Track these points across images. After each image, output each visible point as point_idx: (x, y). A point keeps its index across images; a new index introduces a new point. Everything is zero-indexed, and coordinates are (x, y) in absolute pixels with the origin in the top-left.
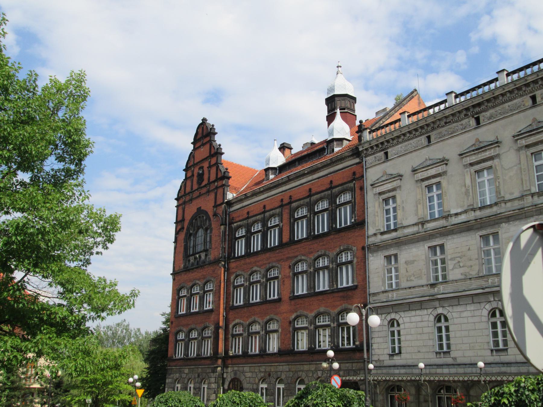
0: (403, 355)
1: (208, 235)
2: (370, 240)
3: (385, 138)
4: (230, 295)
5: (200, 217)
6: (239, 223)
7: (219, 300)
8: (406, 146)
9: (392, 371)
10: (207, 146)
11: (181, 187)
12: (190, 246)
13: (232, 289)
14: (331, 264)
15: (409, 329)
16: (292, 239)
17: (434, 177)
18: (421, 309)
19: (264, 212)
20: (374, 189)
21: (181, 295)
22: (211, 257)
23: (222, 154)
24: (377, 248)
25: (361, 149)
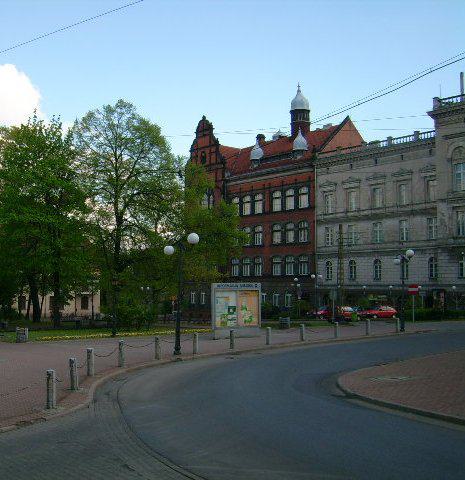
24: (320, 222)
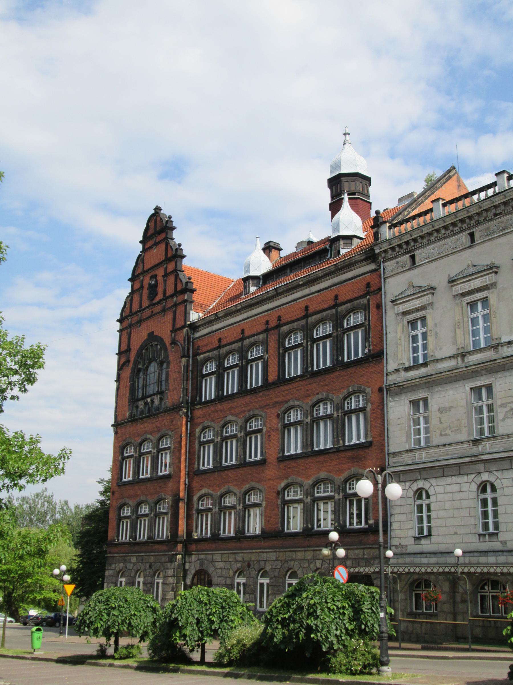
0: (433, 539)
1: (164, 371)
2: (390, 378)
3: (411, 236)
4: (194, 455)
5: (152, 346)
6: (207, 354)
7: (180, 462)
8: (440, 247)
9: (417, 560)
10: (163, 246)
11: (125, 303)
12: (138, 387)
13: (197, 447)
14: (335, 412)
15: (443, 503)
16: (281, 376)
18: (460, 474)
19: (242, 339)
20: (396, 307)
21: (125, 455)
22: (168, 402)
23: (184, 257)
25: (377, 251)
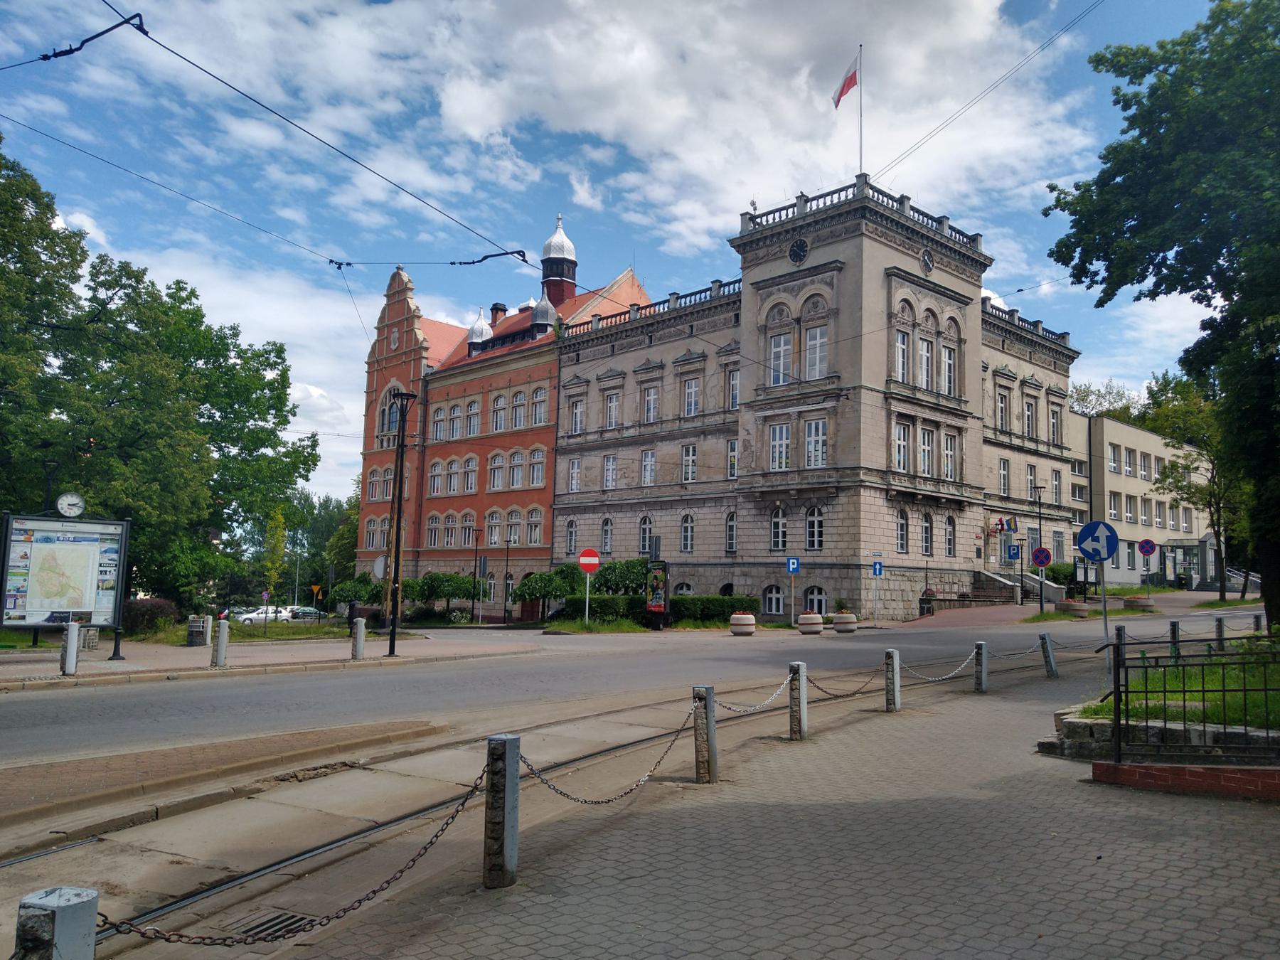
17: (614, 388)
